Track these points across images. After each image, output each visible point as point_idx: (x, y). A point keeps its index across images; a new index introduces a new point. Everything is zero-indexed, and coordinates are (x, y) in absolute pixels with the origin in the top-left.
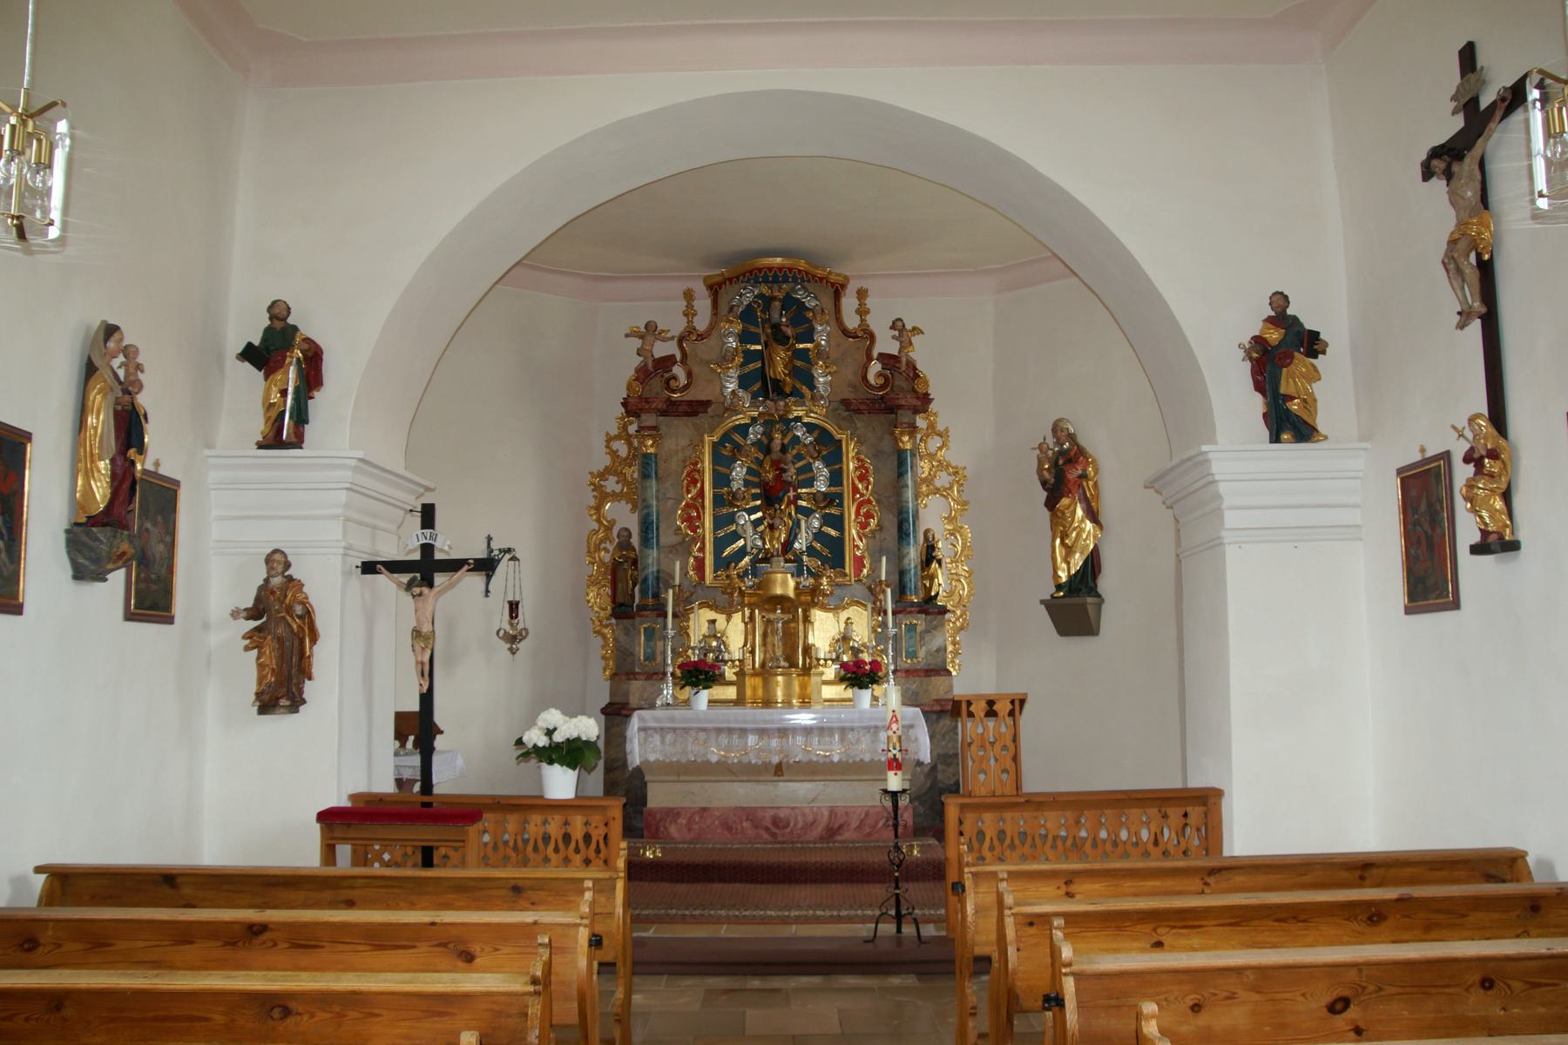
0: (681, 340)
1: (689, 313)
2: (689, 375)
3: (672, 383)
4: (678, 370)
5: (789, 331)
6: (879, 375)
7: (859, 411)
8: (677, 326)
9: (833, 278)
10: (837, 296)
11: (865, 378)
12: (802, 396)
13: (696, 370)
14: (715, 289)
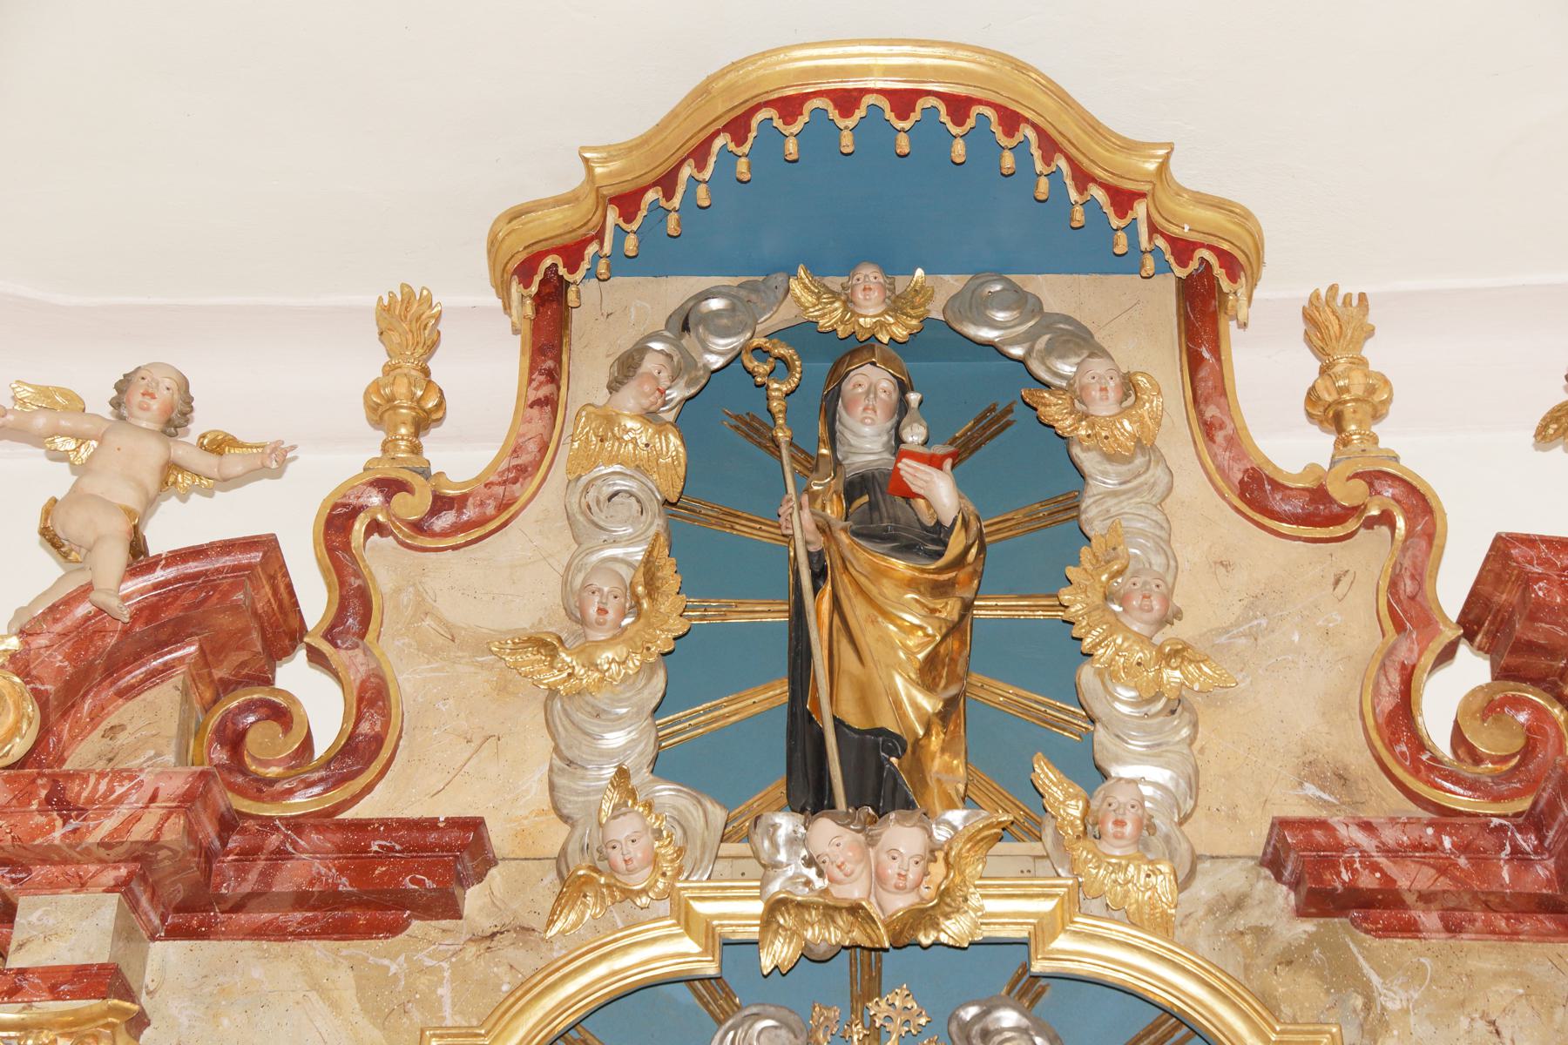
0: (337, 523)
1: (408, 408)
2: (371, 698)
3: (262, 740)
4: (295, 676)
5: (940, 492)
6: (1489, 707)
7: (1378, 908)
8: (340, 458)
9: (1189, 221)
10: (1202, 309)
11: (1401, 718)
12: (1029, 822)
13: (410, 682)
14: (543, 279)
